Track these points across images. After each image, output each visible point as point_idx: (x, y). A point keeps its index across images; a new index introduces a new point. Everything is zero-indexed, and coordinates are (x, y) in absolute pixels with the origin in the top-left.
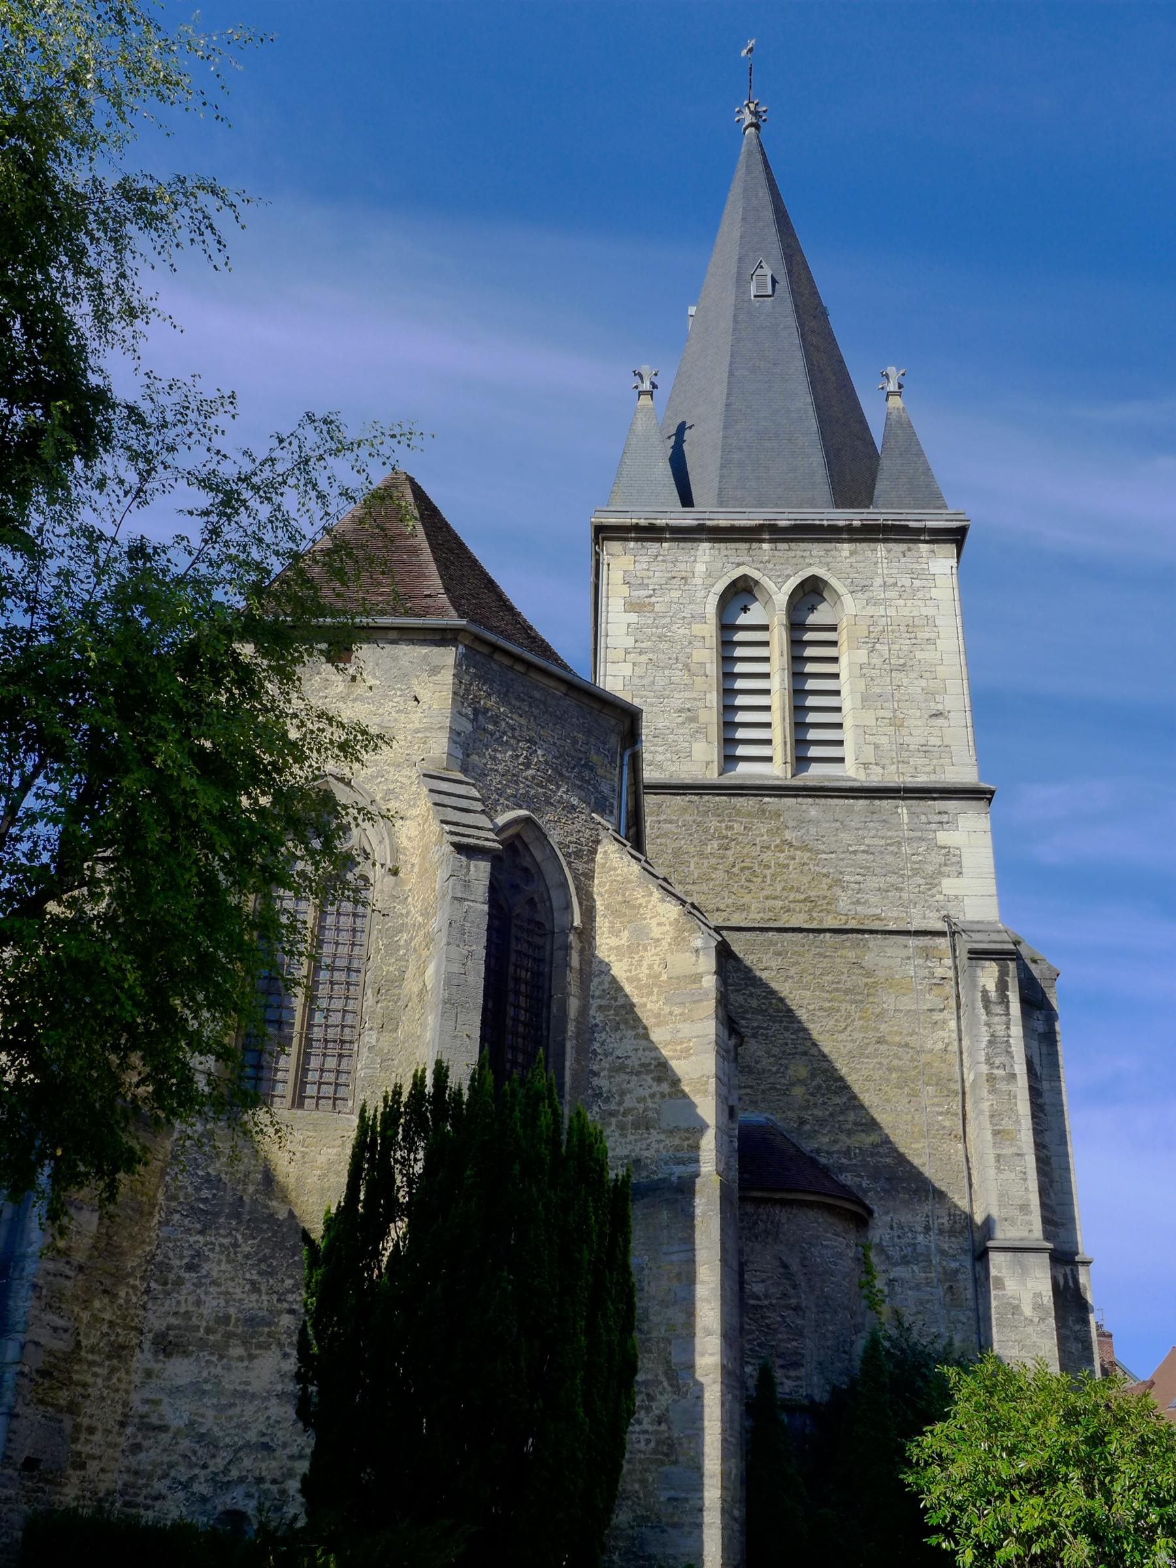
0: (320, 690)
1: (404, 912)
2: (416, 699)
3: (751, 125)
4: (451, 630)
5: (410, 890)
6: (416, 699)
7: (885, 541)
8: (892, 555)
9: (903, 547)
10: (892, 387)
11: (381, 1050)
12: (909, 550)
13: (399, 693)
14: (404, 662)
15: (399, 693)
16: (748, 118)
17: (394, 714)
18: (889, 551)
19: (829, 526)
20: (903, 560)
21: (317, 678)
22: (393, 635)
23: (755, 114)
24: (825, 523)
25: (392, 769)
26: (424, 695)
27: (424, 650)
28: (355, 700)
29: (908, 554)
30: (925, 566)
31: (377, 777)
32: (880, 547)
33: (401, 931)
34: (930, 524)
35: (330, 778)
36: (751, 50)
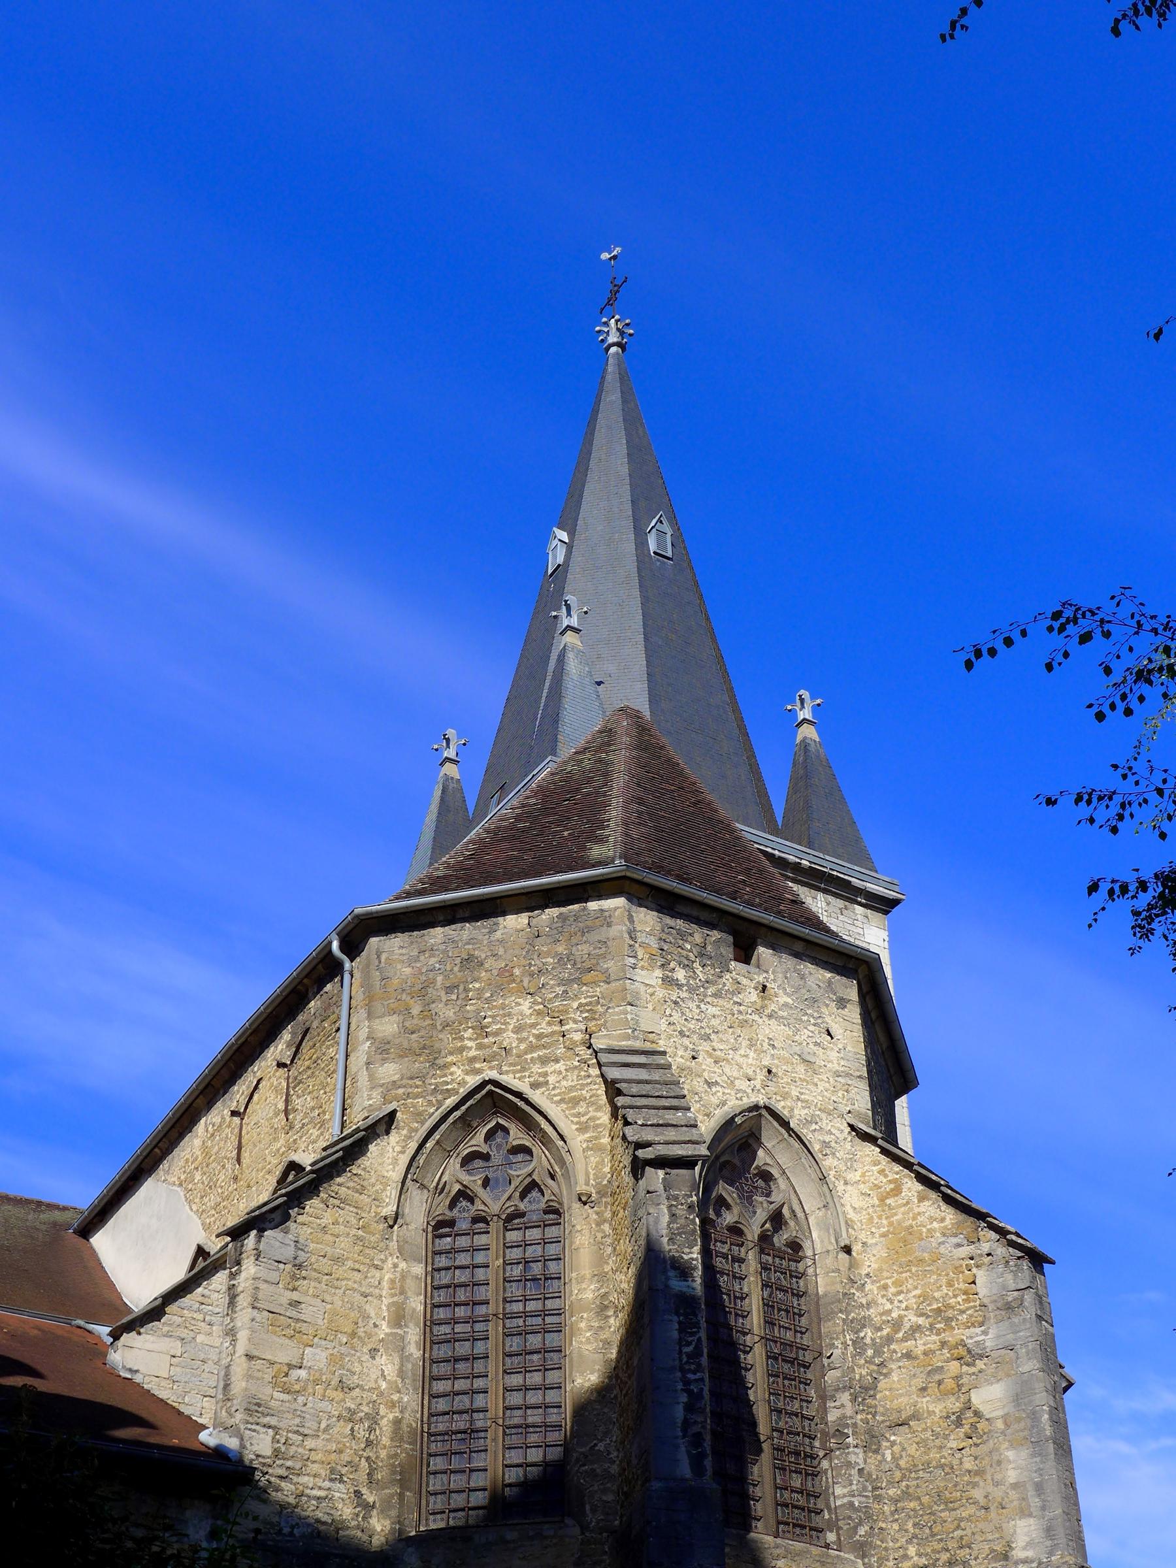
0: (733, 993)
1: (864, 1301)
2: (829, 1034)
3: (618, 344)
4: (857, 959)
5: (868, 1275)
6: (829, 1034)
7: (825, 891)
9: (840, 903)
10: (805, 713)
11: (870, 1475)
13: (812, 1021)
14: (811, 982)
16: (613, 338)
17: (811, 1046)
18: (828, 904)
19: (780, 858)
22: (799, 947)
23: (621, 333)
24: (776, 852)
25: (823, 1116)
26: (836, 1030)
27: (828, 975)
28: (770, 1016)
29: (845, 912)
31: (811, 1122)
32: (820, 895)
33: (864, 1326)
35: (764, 1112)
36: (615, 257)
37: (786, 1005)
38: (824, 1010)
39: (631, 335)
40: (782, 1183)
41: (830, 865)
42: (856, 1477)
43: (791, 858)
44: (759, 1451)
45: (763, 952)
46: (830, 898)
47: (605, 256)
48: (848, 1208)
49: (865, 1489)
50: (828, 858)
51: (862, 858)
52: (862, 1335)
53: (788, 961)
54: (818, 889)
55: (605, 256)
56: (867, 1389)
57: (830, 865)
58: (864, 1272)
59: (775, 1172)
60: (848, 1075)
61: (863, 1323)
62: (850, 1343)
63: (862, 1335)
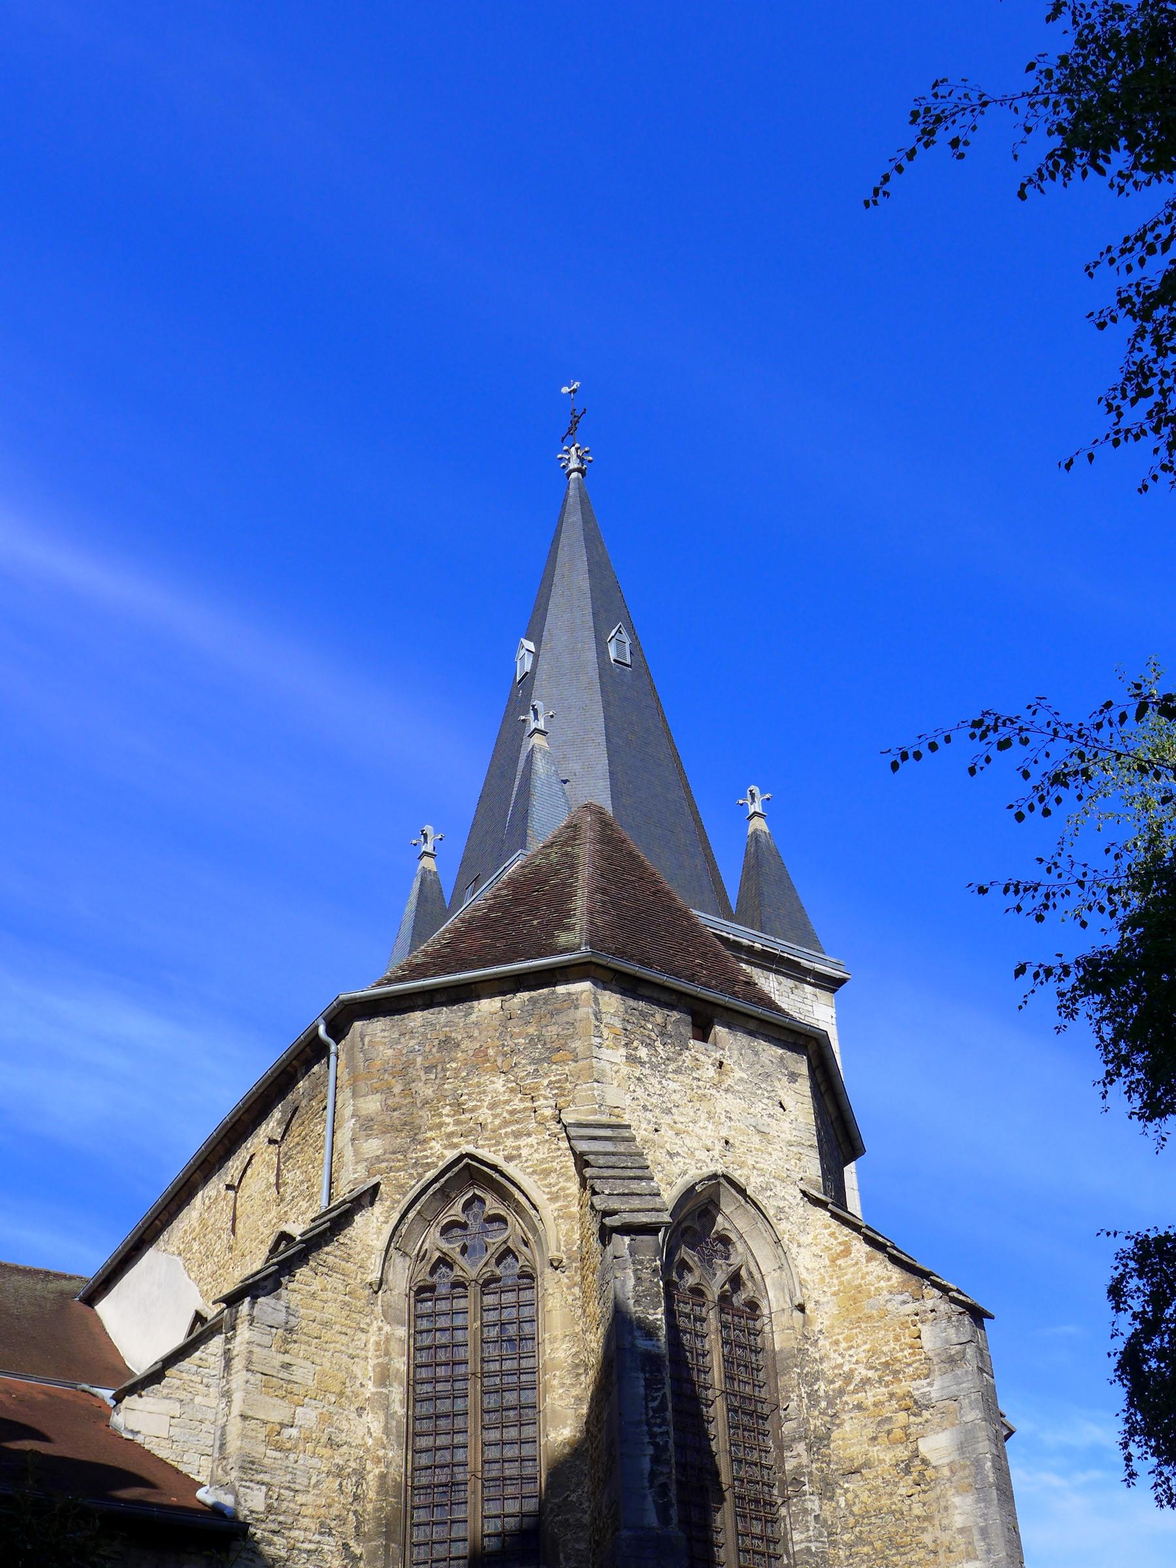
0: (692, 1069)
2: (782, 1106)
3: (578, 470)
4: (807, 1036)
6: (782, 1106)
7: (777, 972)
8: (782, 988)
9: (790, 983)
11: (825, 1521)
12: (796, 987)
13: (766, 1095)
15: (766, 1095)
17: (765, 1117)
18: (780, 984)
19: (734, 941)
20: (792, 996)
21: (687, 1053)
22: (752, 1025)
24: (731, 936)
25: (778, 1183)
27: (780, 1051)
28: (727, 1091)
29: (795, 991)
30: (810, 1009)
32: (772, 976)
33: (818, 1380)
34: (819, 968)
35: (722, 1180)
36: (574, 391)
37: (741, 1079)
38: (776, 1083)
39: (590, 461)
40: (740, 1247)
41: (781, 948)
42: (813, 1523)
43: (745, 942)
44: (722, 1499)
45: (719, 1030)
46: (781, 978)
47: (565, 390)
48: (801, 1270)
49: (821, 1534)
50: (778, 941)
51: (809, 939)
52: (816, 1387)
53: (743, 1039)
54: (770, 970)
55: (565, 390)
56: (821, 1439)
57: (781, 948)
58: (817, 1329)
59: (733, 1236)
60: (800, 1144)
61: (817, 1377)
62: (804, 1395)
63: (816, 1387)
